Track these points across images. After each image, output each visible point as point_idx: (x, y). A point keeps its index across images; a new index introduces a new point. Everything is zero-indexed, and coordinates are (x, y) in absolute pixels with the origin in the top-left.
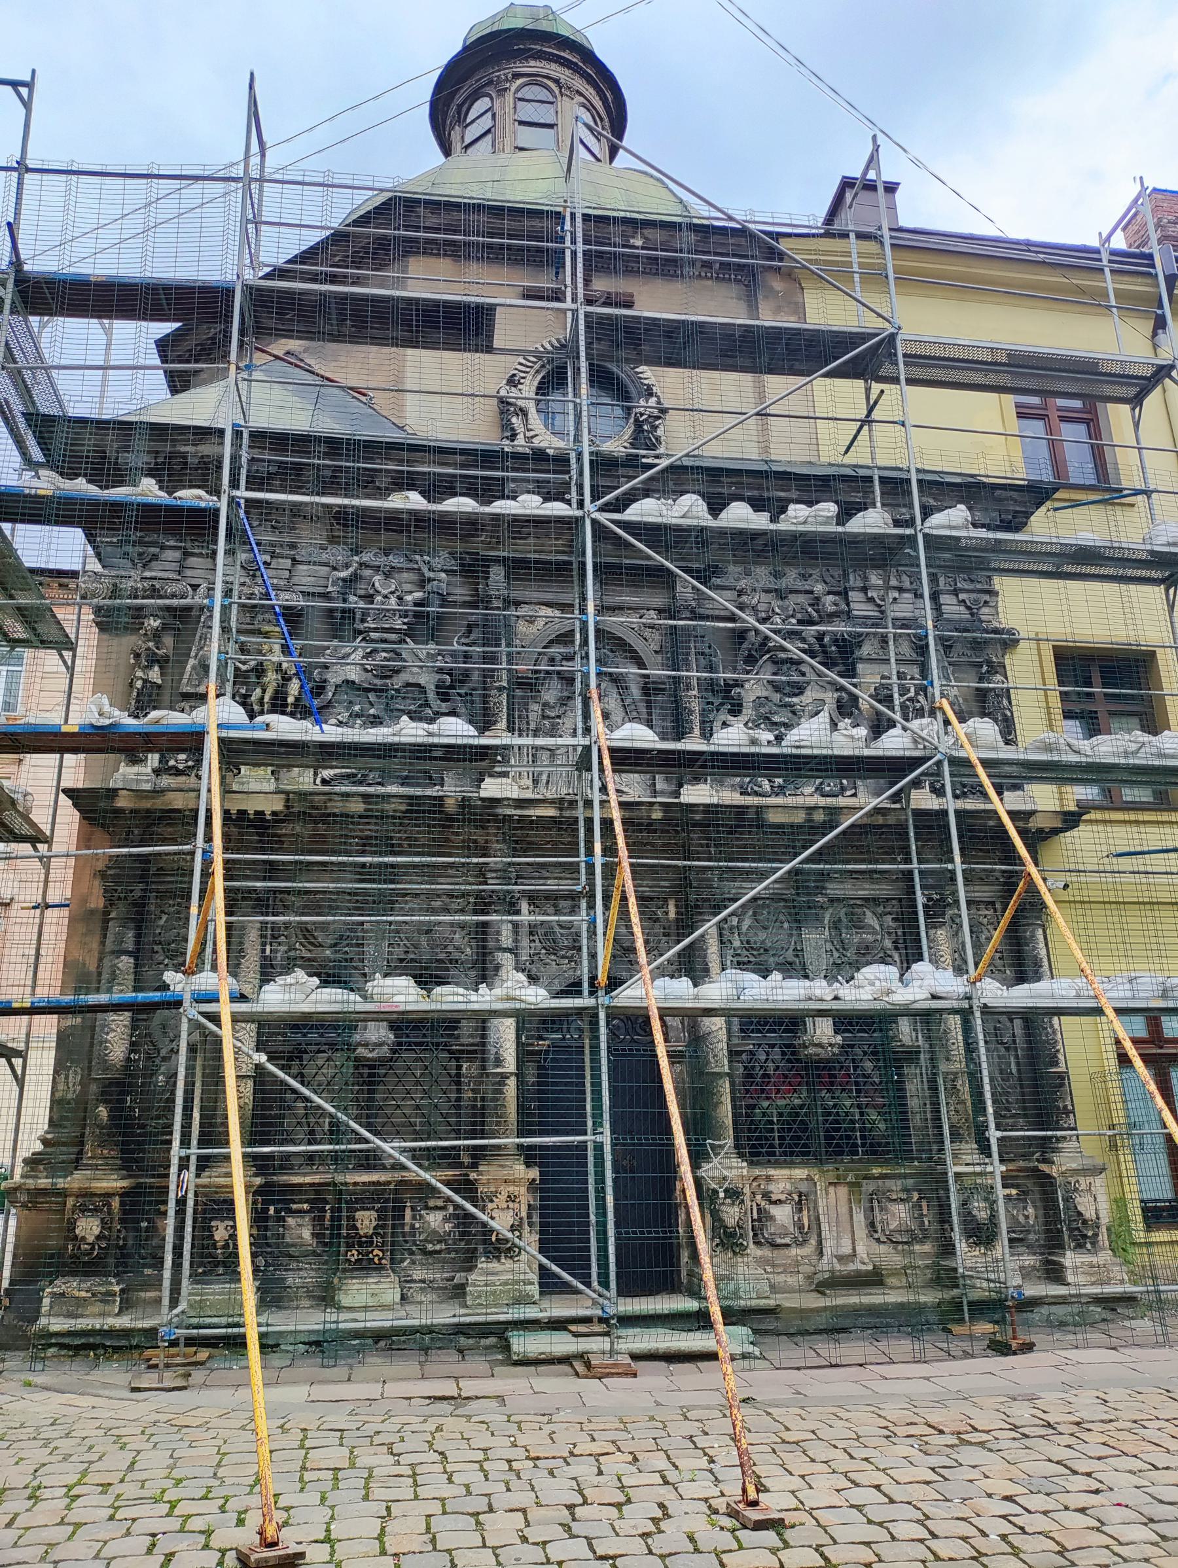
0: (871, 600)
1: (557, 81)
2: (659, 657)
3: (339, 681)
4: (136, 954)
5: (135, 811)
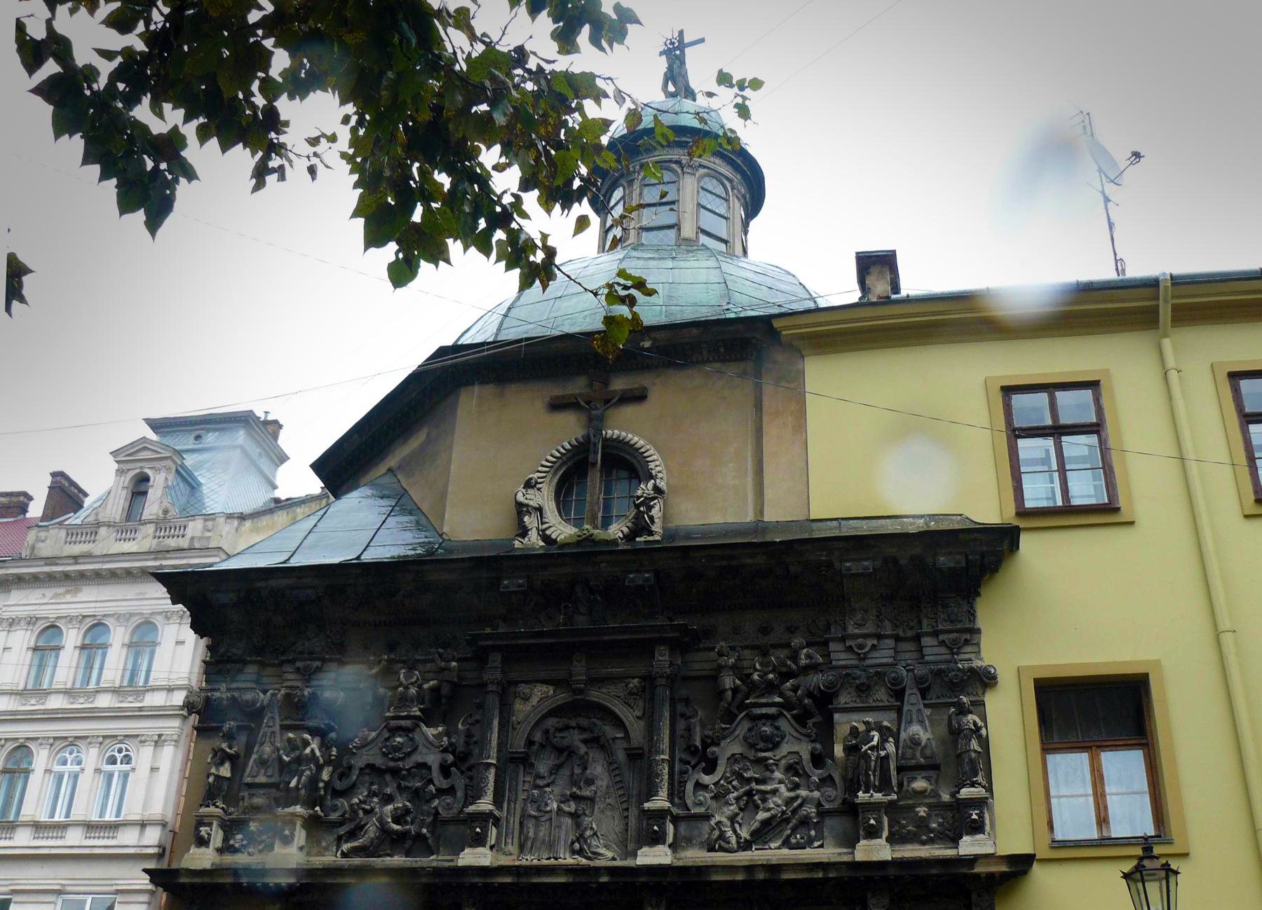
0: (850, 649)
1: (678, 162)
2: (642, 723)
5: (193, 885)
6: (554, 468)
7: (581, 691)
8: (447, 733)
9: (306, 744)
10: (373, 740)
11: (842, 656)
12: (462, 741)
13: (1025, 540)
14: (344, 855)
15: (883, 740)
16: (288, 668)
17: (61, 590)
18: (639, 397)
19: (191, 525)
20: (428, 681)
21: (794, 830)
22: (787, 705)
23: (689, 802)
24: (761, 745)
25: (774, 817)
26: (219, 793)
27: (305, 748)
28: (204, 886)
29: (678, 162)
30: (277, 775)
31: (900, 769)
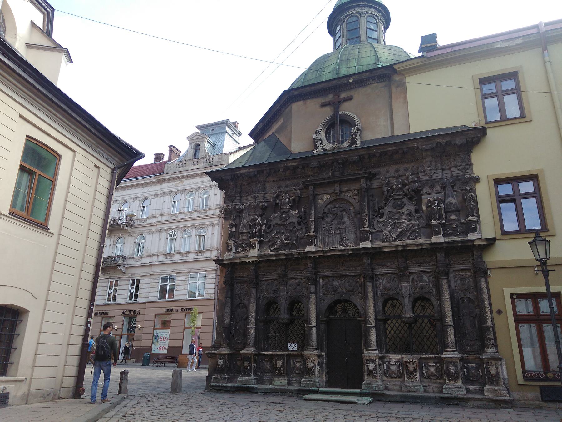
4: (232, 298)
5: (228, 263)
6: (324, 126)
7: (338, 196)
8: (298, 212)
11: (424, 177)
13: (488, 131)
14: (271, 251)
15: (439, 203)
16: (249, 197)
17: (178, 182)
18: (350, 99)
19: (214, 158)
21: (410, 234)
22: (406, 195)
23: (375, 227)
24: (398, 208)
25: (403, 230)
26: (232, 236)
28: (231, 263)
29: (359, 13)
31: (446, 213)
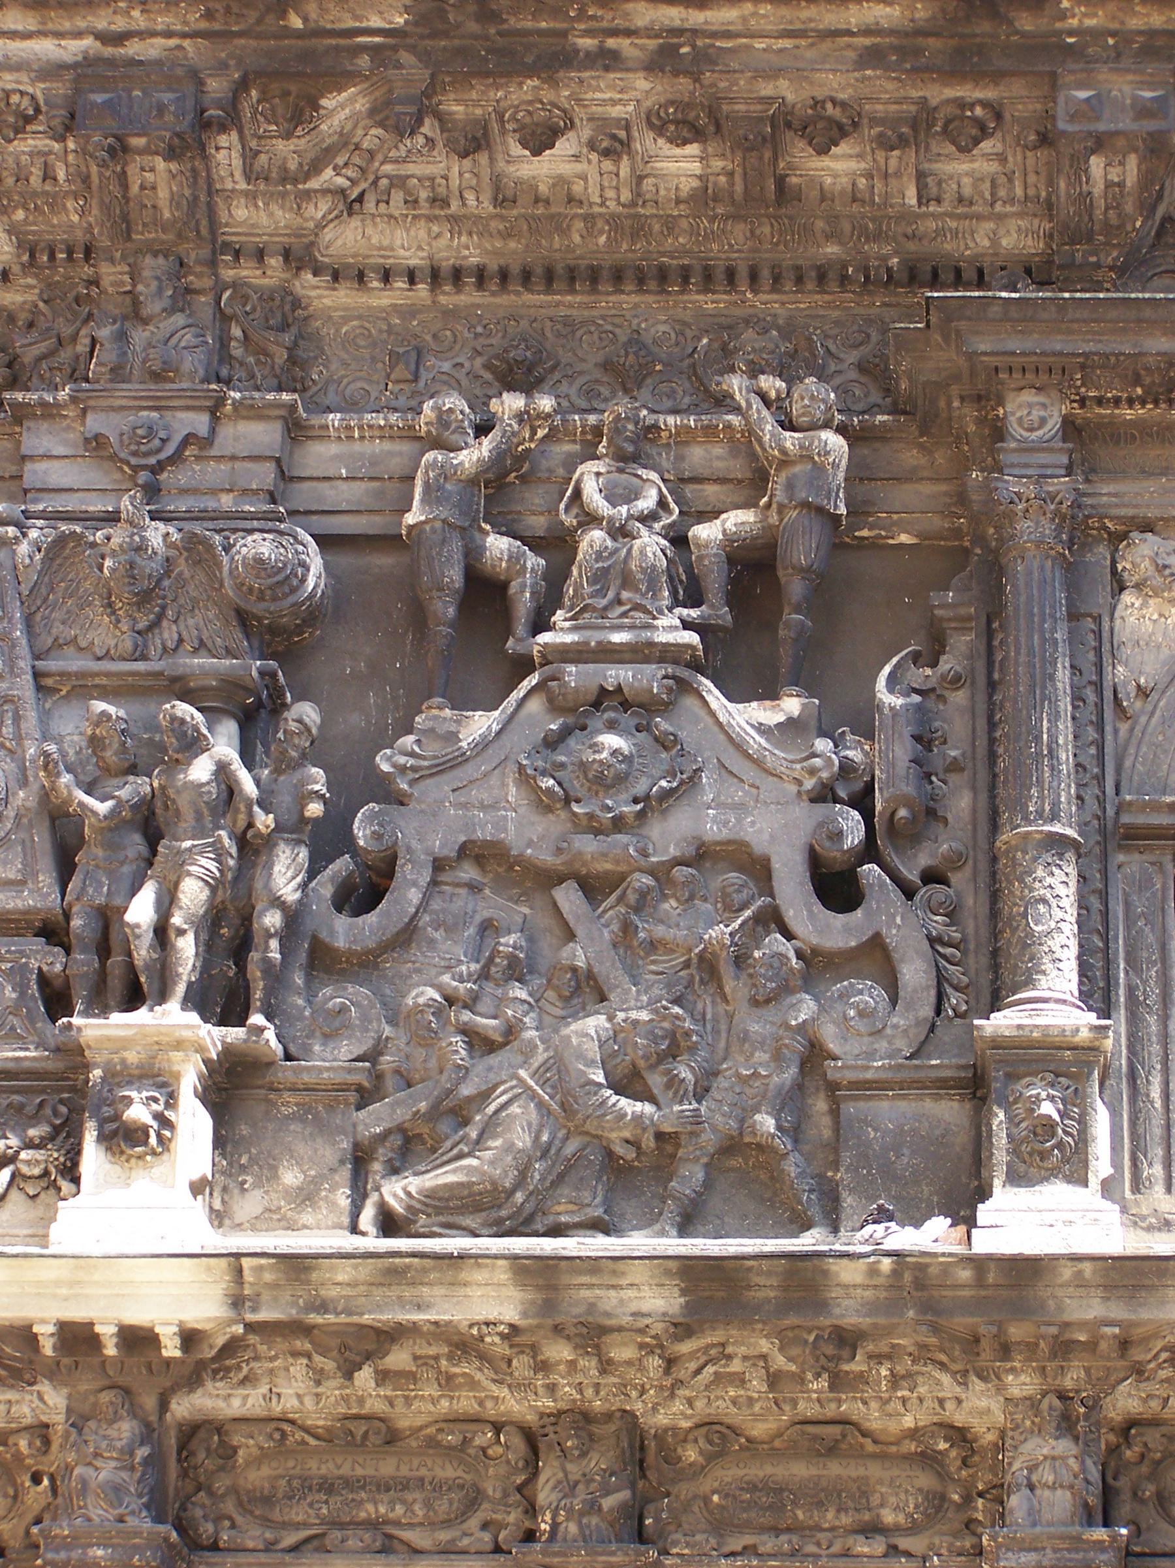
3: (441, 842)
9: (193, 745)
10: (484, 745)
12: (903, 751)
16: (39, 438)
20: (715, 514)
27: (180, 763)
30: (47, 879)
